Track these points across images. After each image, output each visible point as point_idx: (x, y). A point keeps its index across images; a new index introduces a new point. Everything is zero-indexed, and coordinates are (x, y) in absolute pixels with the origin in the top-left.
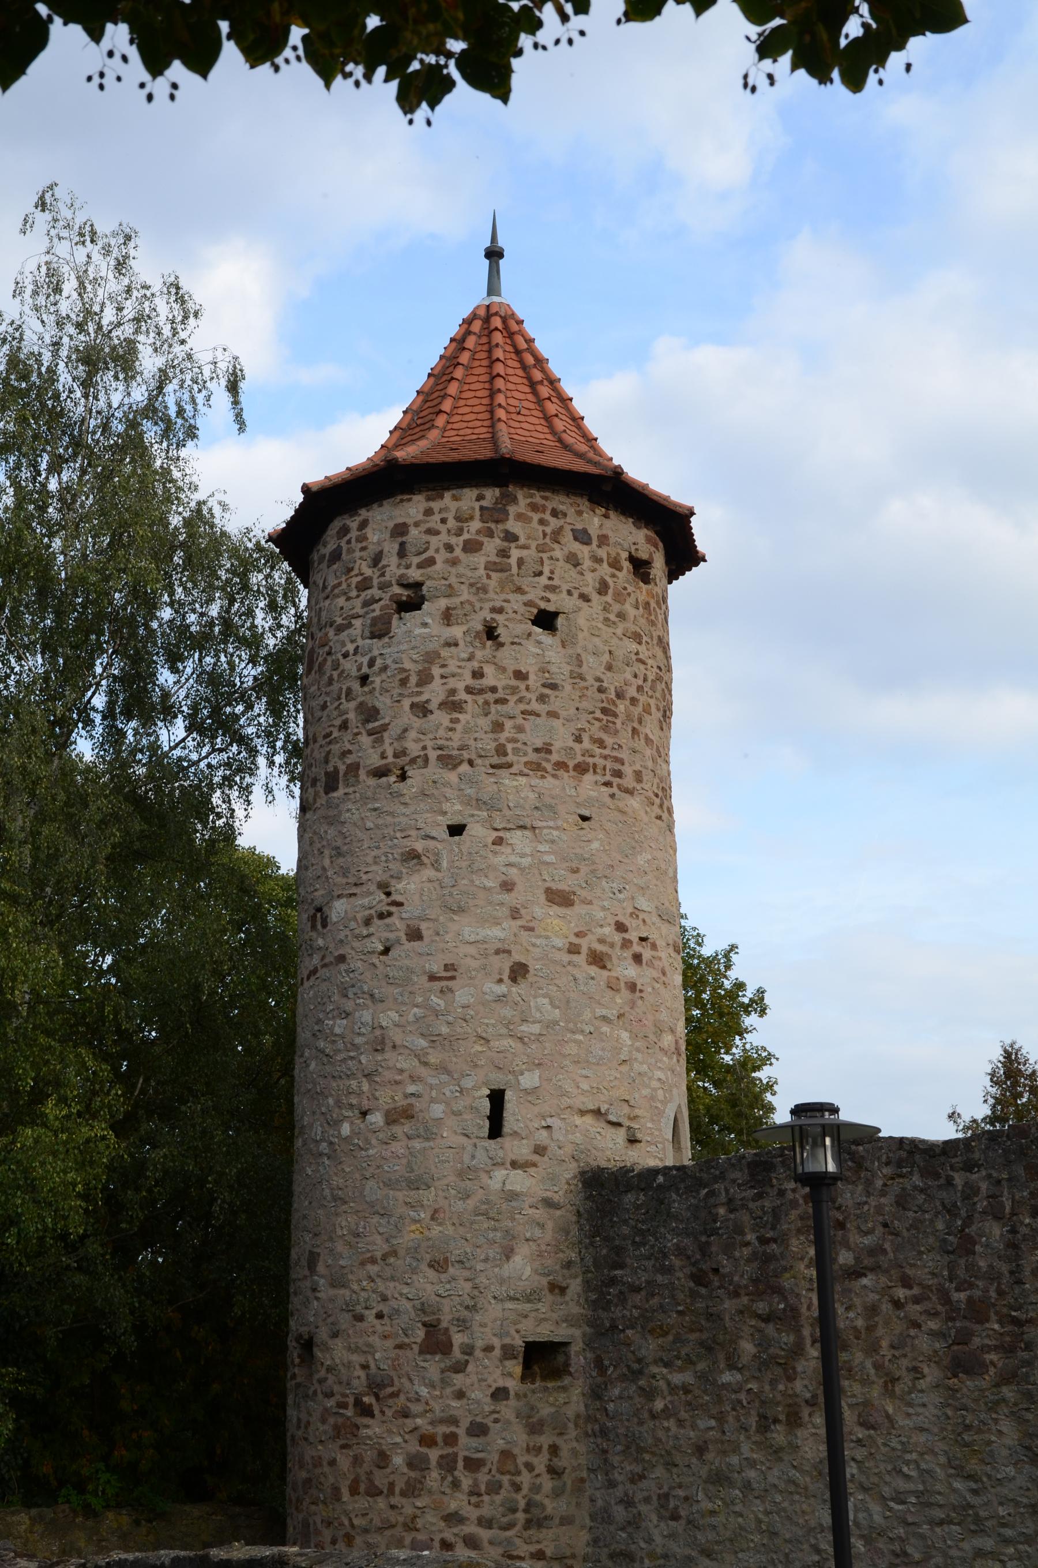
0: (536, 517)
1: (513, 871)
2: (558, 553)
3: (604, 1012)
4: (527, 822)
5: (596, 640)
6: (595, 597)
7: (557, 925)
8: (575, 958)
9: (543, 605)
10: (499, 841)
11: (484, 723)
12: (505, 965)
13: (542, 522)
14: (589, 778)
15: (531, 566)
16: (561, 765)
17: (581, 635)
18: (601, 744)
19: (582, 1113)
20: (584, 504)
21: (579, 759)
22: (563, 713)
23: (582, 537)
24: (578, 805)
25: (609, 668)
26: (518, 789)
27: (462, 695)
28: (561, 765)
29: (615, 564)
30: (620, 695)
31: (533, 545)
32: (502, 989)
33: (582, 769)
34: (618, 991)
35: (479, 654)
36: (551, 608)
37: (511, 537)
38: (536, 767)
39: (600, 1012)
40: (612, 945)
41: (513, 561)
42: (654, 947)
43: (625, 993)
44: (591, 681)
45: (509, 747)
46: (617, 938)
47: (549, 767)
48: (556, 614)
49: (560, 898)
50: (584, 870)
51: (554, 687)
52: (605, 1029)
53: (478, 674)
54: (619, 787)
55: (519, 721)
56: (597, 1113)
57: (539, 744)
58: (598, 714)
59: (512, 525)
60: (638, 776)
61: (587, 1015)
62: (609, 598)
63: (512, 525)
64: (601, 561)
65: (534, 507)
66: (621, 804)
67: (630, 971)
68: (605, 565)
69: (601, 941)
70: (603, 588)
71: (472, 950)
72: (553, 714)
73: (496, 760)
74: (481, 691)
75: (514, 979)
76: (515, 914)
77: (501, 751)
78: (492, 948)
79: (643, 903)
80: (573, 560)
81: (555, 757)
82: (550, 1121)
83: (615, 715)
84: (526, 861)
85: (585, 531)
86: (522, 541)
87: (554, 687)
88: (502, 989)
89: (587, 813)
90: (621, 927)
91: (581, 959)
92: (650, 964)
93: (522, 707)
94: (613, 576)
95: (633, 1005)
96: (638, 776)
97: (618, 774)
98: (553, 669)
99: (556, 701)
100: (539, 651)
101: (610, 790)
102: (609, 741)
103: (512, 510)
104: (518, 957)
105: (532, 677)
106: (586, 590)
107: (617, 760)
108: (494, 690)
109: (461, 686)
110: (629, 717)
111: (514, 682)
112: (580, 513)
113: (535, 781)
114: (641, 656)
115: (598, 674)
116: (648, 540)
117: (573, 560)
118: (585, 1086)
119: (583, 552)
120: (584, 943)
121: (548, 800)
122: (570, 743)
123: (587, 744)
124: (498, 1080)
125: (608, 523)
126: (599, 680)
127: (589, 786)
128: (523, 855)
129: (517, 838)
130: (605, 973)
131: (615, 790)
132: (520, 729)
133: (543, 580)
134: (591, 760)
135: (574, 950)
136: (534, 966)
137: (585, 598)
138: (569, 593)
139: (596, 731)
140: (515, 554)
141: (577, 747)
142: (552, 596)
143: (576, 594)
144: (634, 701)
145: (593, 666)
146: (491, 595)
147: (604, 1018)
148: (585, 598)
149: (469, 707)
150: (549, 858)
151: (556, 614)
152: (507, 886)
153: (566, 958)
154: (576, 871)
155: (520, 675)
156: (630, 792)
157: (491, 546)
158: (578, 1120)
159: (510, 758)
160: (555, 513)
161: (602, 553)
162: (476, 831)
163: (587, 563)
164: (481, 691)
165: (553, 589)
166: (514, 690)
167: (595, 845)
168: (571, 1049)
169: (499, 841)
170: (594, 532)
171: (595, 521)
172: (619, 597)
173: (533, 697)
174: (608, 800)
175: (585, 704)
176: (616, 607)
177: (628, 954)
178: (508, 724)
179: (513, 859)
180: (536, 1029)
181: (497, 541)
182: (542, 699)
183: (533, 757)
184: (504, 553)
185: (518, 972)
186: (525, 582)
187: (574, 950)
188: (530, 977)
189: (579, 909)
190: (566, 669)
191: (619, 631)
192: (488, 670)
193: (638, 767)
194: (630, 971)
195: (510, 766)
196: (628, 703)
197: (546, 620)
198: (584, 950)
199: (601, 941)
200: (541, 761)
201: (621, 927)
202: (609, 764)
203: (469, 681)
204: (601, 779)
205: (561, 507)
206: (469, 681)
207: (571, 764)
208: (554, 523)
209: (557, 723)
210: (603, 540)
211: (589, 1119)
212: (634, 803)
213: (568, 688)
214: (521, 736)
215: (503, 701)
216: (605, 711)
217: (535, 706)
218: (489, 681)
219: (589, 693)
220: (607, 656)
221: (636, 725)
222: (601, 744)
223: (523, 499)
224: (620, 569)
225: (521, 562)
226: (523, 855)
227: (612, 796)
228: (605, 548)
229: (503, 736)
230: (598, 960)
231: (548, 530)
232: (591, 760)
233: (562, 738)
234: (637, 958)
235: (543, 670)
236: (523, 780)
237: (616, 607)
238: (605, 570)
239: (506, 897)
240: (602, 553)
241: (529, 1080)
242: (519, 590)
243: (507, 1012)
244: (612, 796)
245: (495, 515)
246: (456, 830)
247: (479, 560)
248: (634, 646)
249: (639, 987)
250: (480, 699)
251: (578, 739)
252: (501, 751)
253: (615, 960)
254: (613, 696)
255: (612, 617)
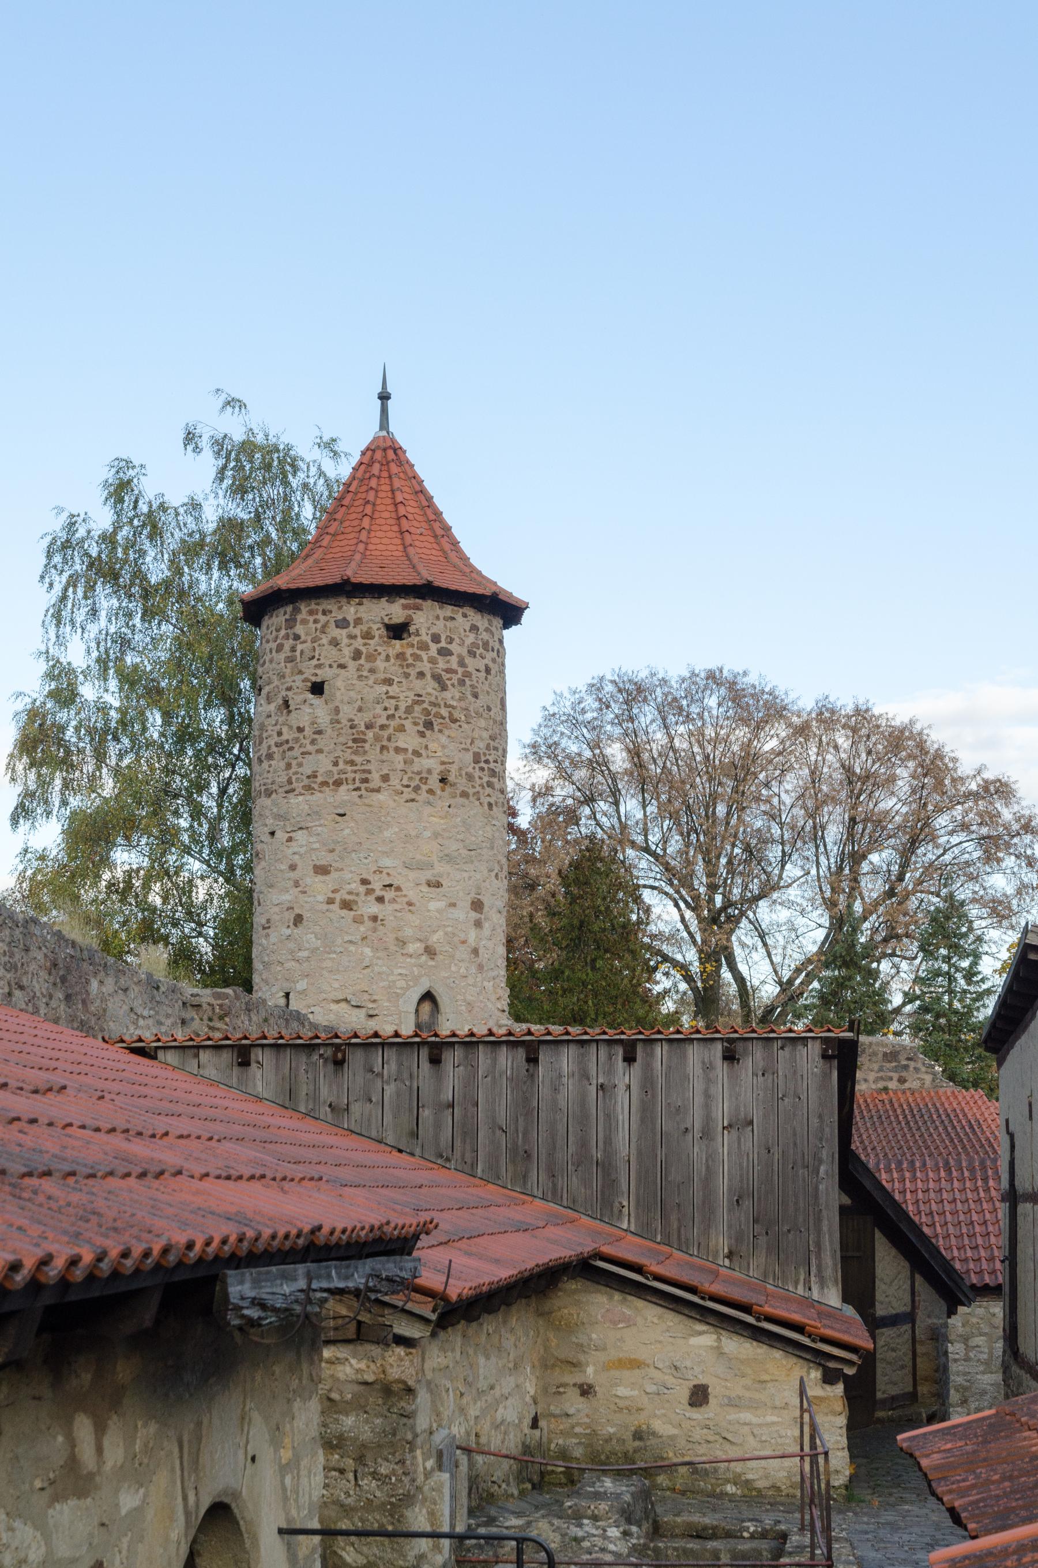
0: (311, 619)
1: (297, 857)
2: (325, 641)
3: (350, 938)
4: (303, 824)
5: (352, 694)
6: (352, 665)
7: (320, 887)
8: (331, 906)
9: (314, 679)
10: (290, 839)
11: (283, 765)
12: (290, 916)
13: (316, 621)
14: (343, 788)
15: (308, 654)
16: (325, 784)
17: (338, 694)
18: (352, 763)
19: (338, 1002)
20: (343, 600)
21: (336, 777)
22: (326, 749)
23: (342, 624)
24: (335, 807)
25: (360, 710)
26: (298, 803)
27: (274, 749)
28: (325, 784)
29: (368, 635)
30: (369, 726)
31: (309, 638)
32: (288, 932)
33: (338, 783)
34: (362, 923)
35: (280, 720)
36: (319, 680)
37: (297, 637)
38: (309, 788)
39: (346, 938)
40: (357, 894)
41: (298, 653)
42: (398, 889)
43: (369, 924)
44: (344, 721)
45: (294, 778)
46: (362, 889)
47: (316, 786)
48: (323, 683)
49: (322, 870)
50: (338, 849)
51: (320, 732)
52: (352, 948)
53: (280, 734)
54: (366, 790)
55: (300, 760)
56: (346, 1000)
57: (309, 773)
58: (350, 744)
59: (299, 629)
60: (385, 778)
61: (339, 941)
62: (362, 661)
63: (299, 629)
64: (356, 637)
65: (311, 613)
66: (366, 801)
67: (374, 909)
68: (359, 639)
69: (350, 893)
70: (357, 655)
71: (276, 909)
72: (320, 751)
73: (288, 788)
74: (281, 744)
75: (295, 925)
76: (297, 884)
77: (290, 782)
78: (285, 906)
79: (386, 862)
80: (335, 643)
81: (320, 779)
82: (313, 1009)
83: (364, 741)
84: (302, 850)
85: (344, 619)
86: (303, 638)
87: (320, 732)
88: (288, 932)
89: (341, 812)
90: (364, 882)
91: (335, 907)
92: (393, 901)
93: (302, 750)
94: (365, 644)
95: (375, 930)
96: (385, 778)
97: (366, 781)
98: (320, 721)
99: (322, 742)
100: (318, 710)
101: (359, 793)
102: (358, 759)
103: (299, 617)
104: (297, 911)
105: (307, 729)
106: (342, 661)
107: (364, 771)
108: (287, 742)
109: (272, 743)
110: (377, 738)
111: (297, 735)
112: (340, 608)
113: (309, 797)
114: (391, 694)
115: (352, 716)
116: (405, 607)
117: (335, 643)
118: (336, 985)
119: (341, 634)
120: (338, 897)
121: (316, 809)
122: (330, 767)
123: (341, 766)
124: (287, 987)
125: (361, 608)
126: (351, 720)
127: (344, 793)
128: (301, 846)
129: (300, 836)
130: (352, 913)
131: (363, 792)
132: (300, 765)
133: (314, 662)
134: (343, 776)
135: (330, 901)
136: (306, 915)
137: (342, 666)
138: (331, 666)
139: (348, 755)
140: (299, 647)
141: (335, 769)
142: (318, 671)
143: (335, 665)
144: (383, 727)
145: (347, 712)
146: (287, 679)
147: (351, 942)
148: (342, 666)
149: (276, 756)
150: (315, 846)
151: (323, 683)
152: (293, 867)
153: (325, 907)
154: (332, 851)
155: (300, 730)
156: (378, 790)
157: (288, 644)
158: (334, 1007)
159: (295, 785)
160: (324, 613)
161: (357, 631)
162: (279, 834)
163: (345, 641)
164: (281, 744)
165: (319, 666)
166: (297, 740)
167: (347, 831)
168: (328, 964)
169: (290, 839)
170: (351, 618)
171: (350, 610)
172: (371, 658)
173: (308, 742)
174: (358, 800)
175: (342, 739)
176: (368, 666)
177: (371, 898)
178: (294, 763)
179: (296, 850)
180: (305, 954)
181: (291, 641)
182: (313, 742)
183: (306, 782)
184: (293, 649)
185: (298, 919)
186: (303, 666)
187: (330, 901)
188: (305, 923)
189: (334, 875)
190: (328, 719)
191: (371, 682)
192: (285, 730)
193: (385, 771)
194: (374, 909)
195: (293, 790)
196: (377, 730)
197: (318, 689)
198: (338, 901)
199: (350, 893)
200: (313, 783)
201: (364, 882)
202: (358, 776)
203: (276, 739)
204: (351, 787)
205: (329, 607)
206: (276, 739)
207: (331, 782)
208: (323, 619)
209: (321, 756)
210: (358, 621)
211: (343, 1005)
212: (381, 797)
213: (329, 731)
214: (300, 770)
215: (291, 749)
216: (355, 741)
217: (310, 748)
218: (285, 737)
219: (343, 731)
220: (359, 703)
221: (385, 743)
222: (352, 763)
223: (304, 608)
224: (373, 638)
225: (302, 652)
226: (301, 846)
227: (360, 797)
228: (360, 627)
229: (291, 772)
230: (347, 905)
231: (319, 626)
232: (343, 776)
233: (323, 764)
234: (380, 900)
235: (313, 723)
236: (301, 798)
237: (368, 666)
238: (359, 643)
239: (292, 875)
240: (357, 631)
241: (301, 985)
242: (300, 672)
243: (291, 945)
244: (360, 797)
245: (291, 623)
246: (272, 834)
247: (282, 656)
248: (384, 688)
249: (380, 917)
250: (281, 749)
251: (336, 764)
252: (290, 782)
253: (360, 904)
254: (363, 728)
255: (365, 673)
